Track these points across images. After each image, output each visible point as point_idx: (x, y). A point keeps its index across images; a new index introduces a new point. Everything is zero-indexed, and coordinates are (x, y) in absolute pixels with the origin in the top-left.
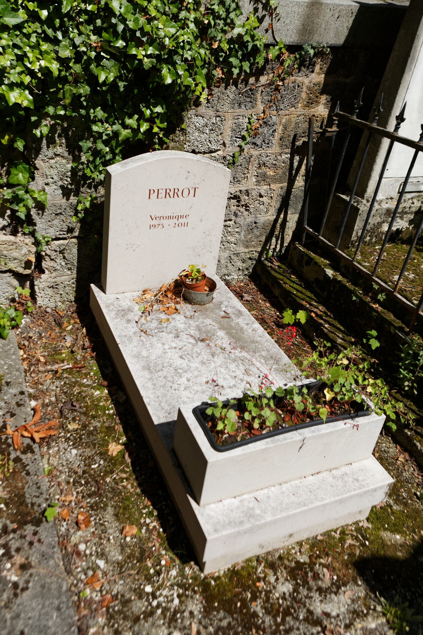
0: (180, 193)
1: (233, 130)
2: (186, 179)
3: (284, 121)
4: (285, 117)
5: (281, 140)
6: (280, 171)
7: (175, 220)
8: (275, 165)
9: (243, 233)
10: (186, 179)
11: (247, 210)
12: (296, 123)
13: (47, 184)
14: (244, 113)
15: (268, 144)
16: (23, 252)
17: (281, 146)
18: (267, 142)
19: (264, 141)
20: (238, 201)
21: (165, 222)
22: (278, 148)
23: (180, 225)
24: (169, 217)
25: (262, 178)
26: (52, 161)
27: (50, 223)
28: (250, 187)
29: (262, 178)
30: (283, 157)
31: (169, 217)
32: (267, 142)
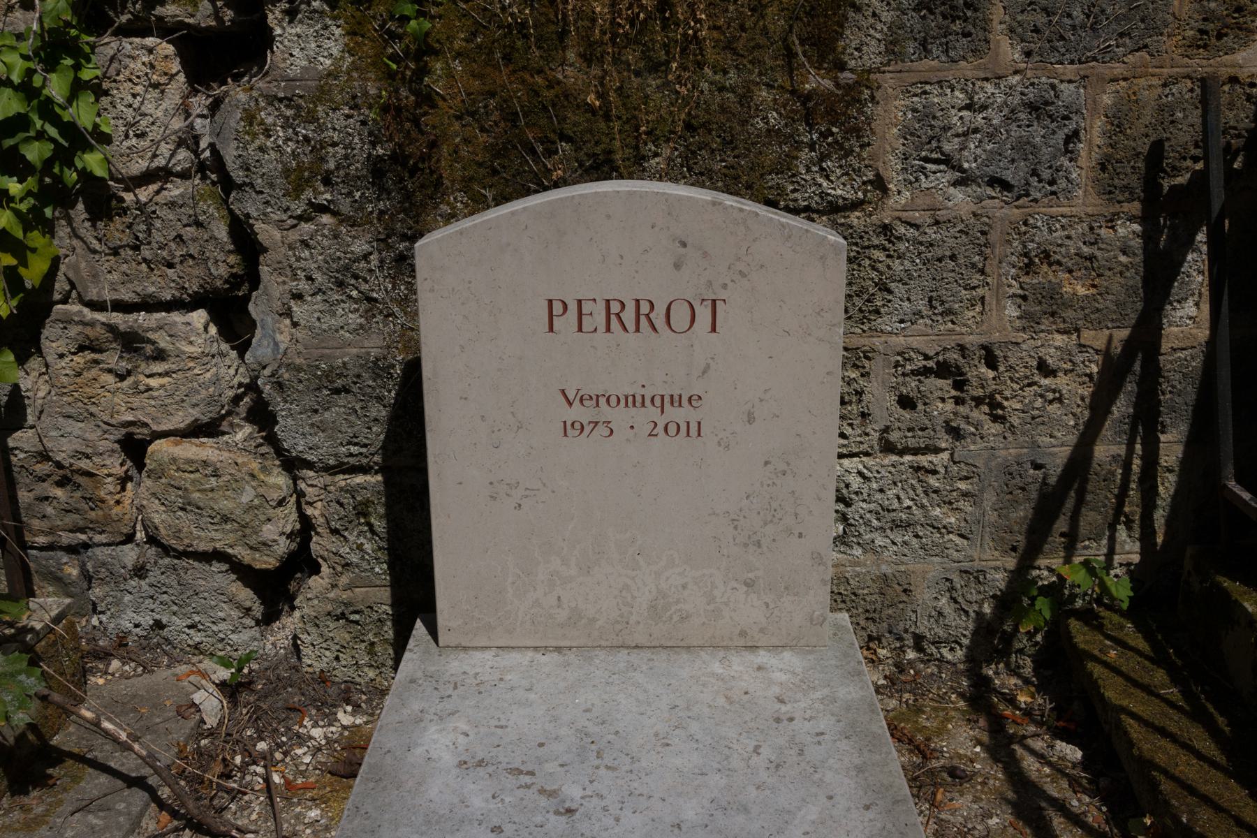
0: (658, 317)
1: (907, 133)
2: (677, 266)
3: (1107, 100)
4: (1111, 88)
5: (1103, 168)
6: (1116, 284)
7: (653, 412)
8: (1091, 258)
9: (989, 498)
10: (677, 266)
11: (996, 419)
12: (1161, 109)
13: (298, 297)
14: (941, 75)
15: (1052, 182)
16: (245, 499)
17: (1108, 192)
18: (1046, 174)
19: (1034, 173)
20: (959, 386)
21: (619, 416)
22: (1094, 199)
23: (672, 429)
24: (632, 401)
25: (1044, 307)
26: (307, 227)
27: (316, 418)
28: (996, 337)
29: (1044, 307)
30: (1121, 231)
31: (632, 401)
32: (1046, 174)
